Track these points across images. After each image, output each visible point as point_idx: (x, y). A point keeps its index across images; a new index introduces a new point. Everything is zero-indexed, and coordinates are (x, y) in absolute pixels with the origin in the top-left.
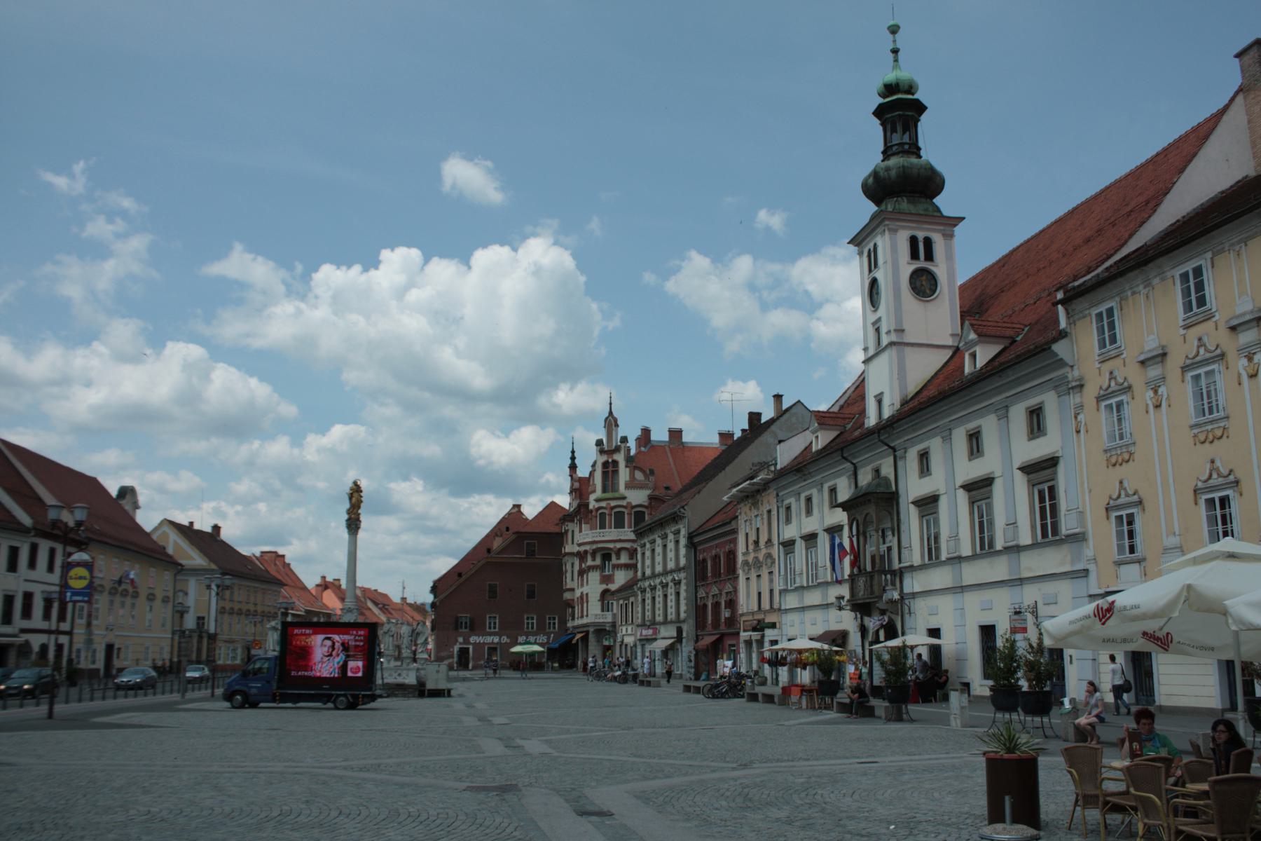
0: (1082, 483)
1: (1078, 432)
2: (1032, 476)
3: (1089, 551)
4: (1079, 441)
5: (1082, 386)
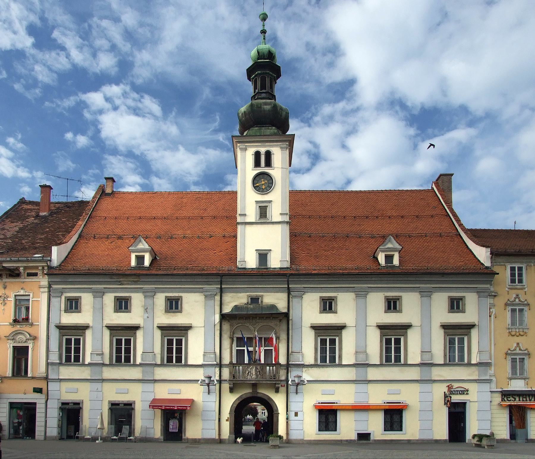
0: (491, 340)
1: (490, 316)
2: (447, 330)
3: (492, 371)
4: (490, 321)
5: (495, 296)
